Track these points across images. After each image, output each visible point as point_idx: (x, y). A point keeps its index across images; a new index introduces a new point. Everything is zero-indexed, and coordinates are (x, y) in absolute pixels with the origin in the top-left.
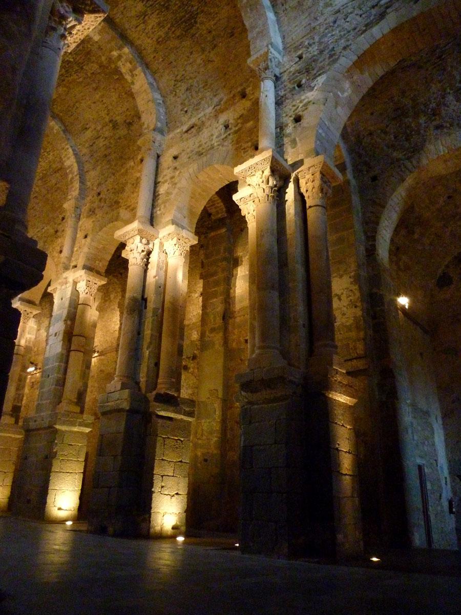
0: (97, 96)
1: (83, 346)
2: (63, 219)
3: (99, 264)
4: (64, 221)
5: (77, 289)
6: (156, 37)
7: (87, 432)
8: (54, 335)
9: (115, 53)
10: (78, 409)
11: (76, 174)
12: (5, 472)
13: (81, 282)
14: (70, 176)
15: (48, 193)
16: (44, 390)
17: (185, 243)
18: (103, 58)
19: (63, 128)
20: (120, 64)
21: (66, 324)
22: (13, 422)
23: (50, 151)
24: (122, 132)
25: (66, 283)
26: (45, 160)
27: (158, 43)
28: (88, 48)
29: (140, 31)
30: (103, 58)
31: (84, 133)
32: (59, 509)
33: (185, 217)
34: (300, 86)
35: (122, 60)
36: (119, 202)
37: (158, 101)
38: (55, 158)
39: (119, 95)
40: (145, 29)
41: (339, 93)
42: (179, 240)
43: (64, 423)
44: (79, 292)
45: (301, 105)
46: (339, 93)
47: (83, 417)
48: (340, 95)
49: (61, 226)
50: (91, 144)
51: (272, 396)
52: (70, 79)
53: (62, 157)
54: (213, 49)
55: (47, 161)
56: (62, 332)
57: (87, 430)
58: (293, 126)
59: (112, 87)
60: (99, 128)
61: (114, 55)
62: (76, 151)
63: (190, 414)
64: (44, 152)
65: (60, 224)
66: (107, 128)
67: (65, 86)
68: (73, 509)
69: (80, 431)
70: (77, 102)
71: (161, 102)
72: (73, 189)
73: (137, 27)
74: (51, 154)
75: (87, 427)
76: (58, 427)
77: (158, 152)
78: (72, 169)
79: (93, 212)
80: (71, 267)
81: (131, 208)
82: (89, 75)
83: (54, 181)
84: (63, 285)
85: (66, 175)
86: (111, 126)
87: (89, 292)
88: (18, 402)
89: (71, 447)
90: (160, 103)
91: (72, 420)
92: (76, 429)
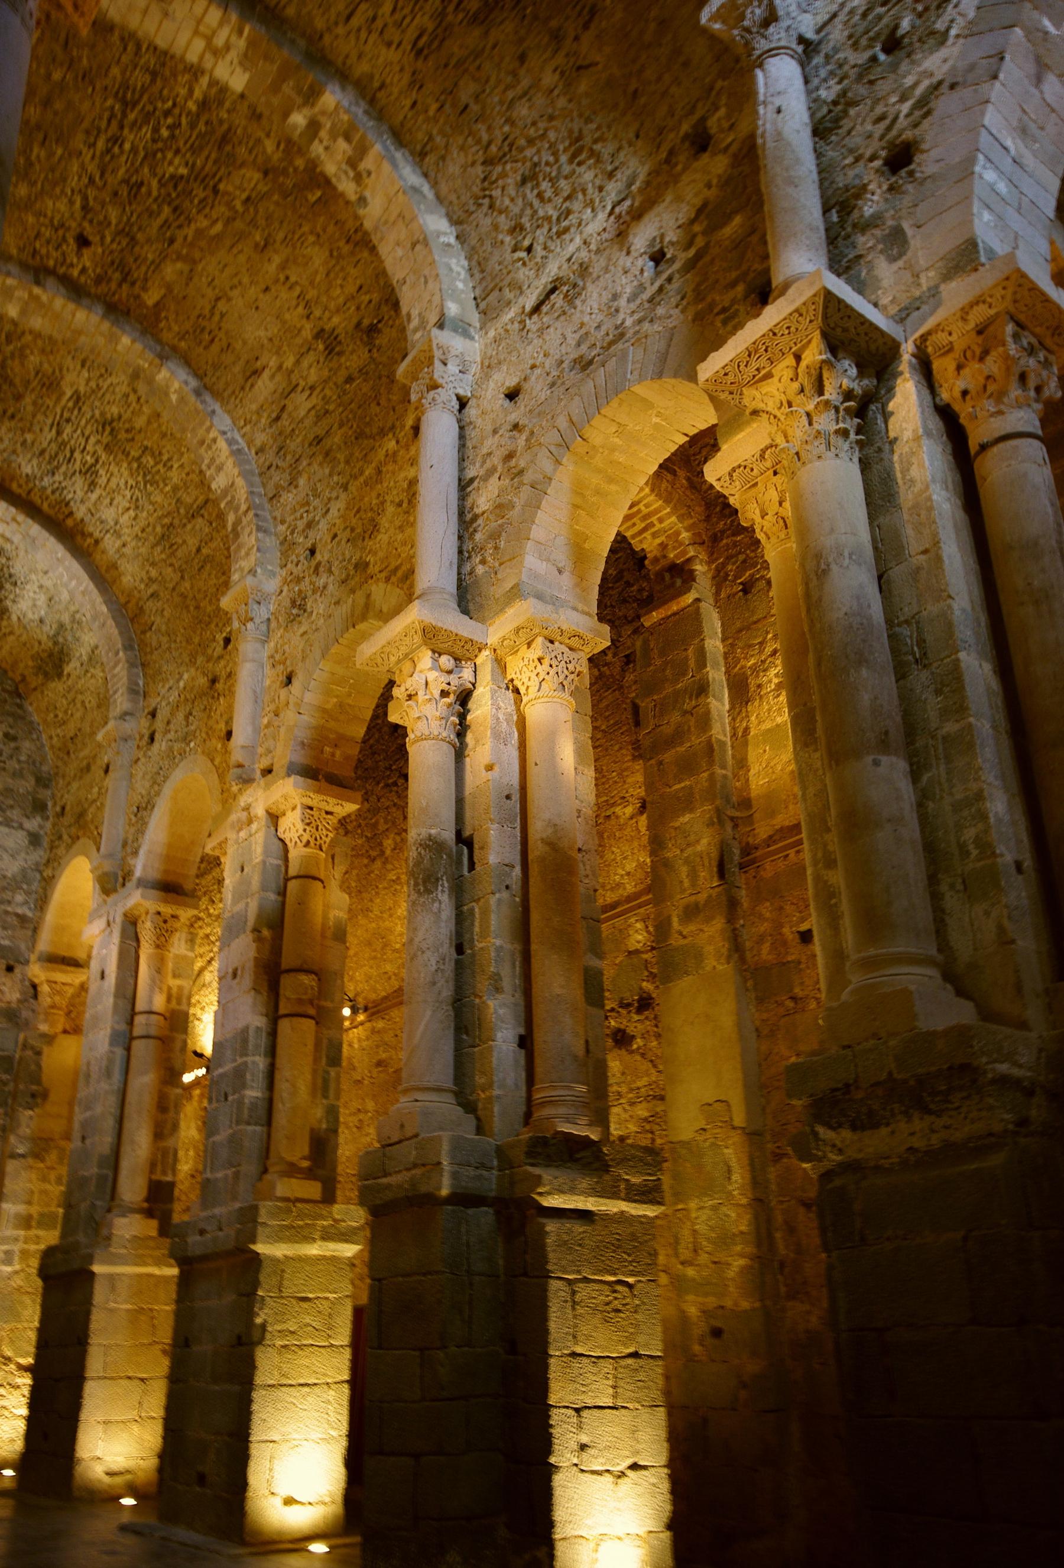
0: (272, 268)
1: (311, 1002)
2: (227, 641)
3: (333, 755)
4: (230, 647)
5: (282, 836)
6: (411, 34)
7: (349, 1254)
8: (230, 976)
9: (298, 119)
10: (313, 1189)
11: (244, 507)
12: (142, 1380)
13: (289, 814)
14: (231, 518)
15: (182, 577)
16: (217, 1138)
17: (571, 649)
18: (269, 146)
19: (193, 383)
20: (317, 149)
21: (259, 940)
22: (154, 1233)
23: (169, 459)
24: (355, 358)
25: (250, 822)
26: (161, 485)
27: (419, 52)
28: (221, 122)
29: (359, 30)
30: (269, 146)
31: (252, 386)
32: (289, 1501)
33: (560, 572)
34: (893, 44)
35: (323, 134)
36: (367, 564)
37: (443, 239)
38: (188, 474)
39: (331, 251)
40: (374, 19)
41: (1047, 23)
42: (552, 642)
43: (282, 1235)
44: (287, 842)
45: (905, 108)
46: (1047, 23)
47: (330, 1213)
48: (1051, 29)
49: (222, 663)
50: (274, 415)
51: (935, 1140)
52: (190, 231)
53: (204, 467)
54: (586, 26)
55: (168, 489)
56: (250, 965)
57: (349, 1250)
58: (885, 187)
59: (306, 228)
60: (289, 363)
61: (295, 126)
62: (237, 443)
63: (648, 1194)
64: (157, 463)
65: (220, 657)
66: (311, 357)
67: (179, 257)
68: (327, 1499)
69: (328, 1254)
70: (218, 299)
71: (452, 240)
72: (243, 552)
73: (349, 18)
74: (176, 466)
75: (347, 1241)
76: (260, 1248)
77: (461, 392)
78: (233, 497)
79: (302, 608)
80: (258, 773)
81: (400, 573)
82: (239, 207)
83: (192, 542)
84: (241, 829)
85: (221, 516)
86: (321, 347)
87: (312, 842)
88: (164, 1173)
89: (305, 1305)
90: (449, 245)
91: (301, 1223)
92: (314, 1250)
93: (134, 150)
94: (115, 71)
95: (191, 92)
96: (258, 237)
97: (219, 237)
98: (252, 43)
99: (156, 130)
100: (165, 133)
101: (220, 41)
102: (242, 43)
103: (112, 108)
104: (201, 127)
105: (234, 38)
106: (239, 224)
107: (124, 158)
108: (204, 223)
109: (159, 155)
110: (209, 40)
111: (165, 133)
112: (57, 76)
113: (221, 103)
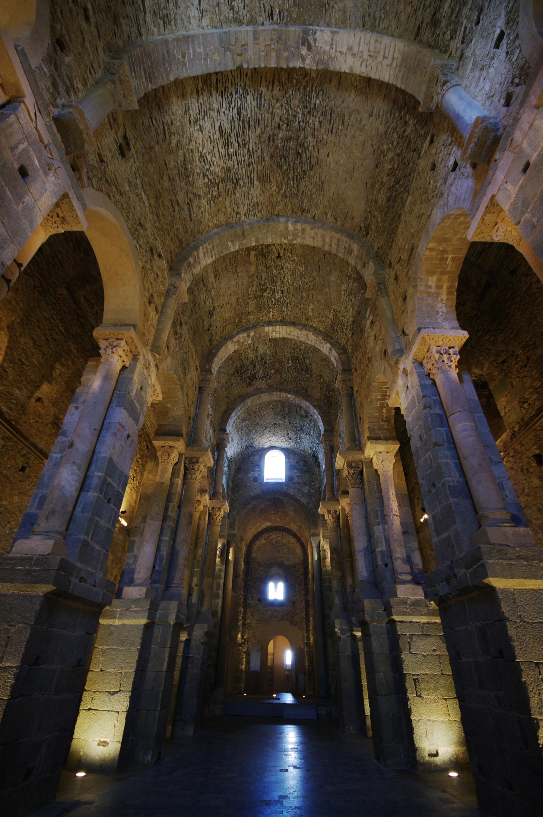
6: (243, 354)
31: (214, 273)
52: (255, 284)
67: (253, 275)
93: (278, 292)
94: (290, 309)
97: (248, 290)
98: (268, 336)
99: (275, 299)
100: (273, 299)
101: (274, 333)
103: (287, 299)
104: (266, 307)
106: (246, 297)
108: (254, 289)
110: (276, 332)
111: (273, 299)
112: (302, 305)
113: (266, 315)
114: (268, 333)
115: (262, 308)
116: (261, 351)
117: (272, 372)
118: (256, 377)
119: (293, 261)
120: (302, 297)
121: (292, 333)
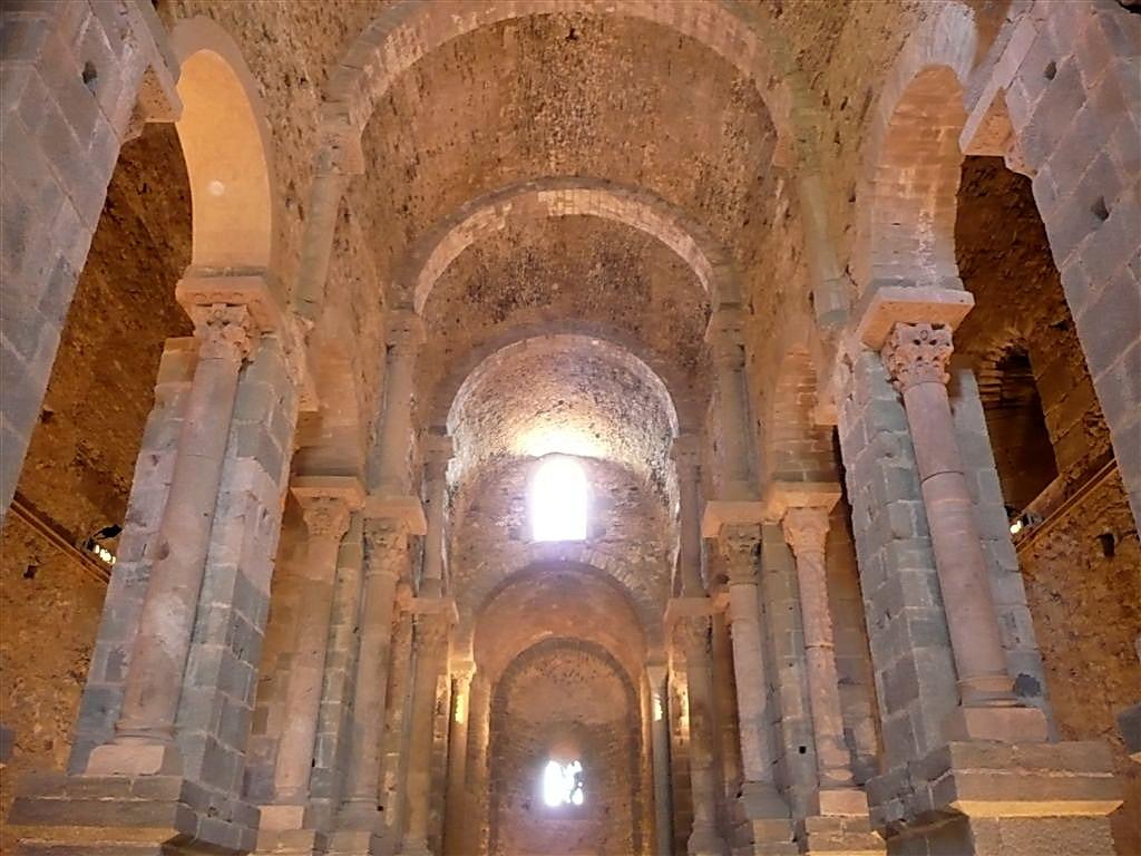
6: (485, 251)
52: (514, 96)
67: (510, 78)
93: (569, 113)
95: (556, 157)
96: (480, 134)
97: (498, 111)
99: (563, 128)
100: (557, 129)
102: (550, 209)
104: (542, 145)
105: (555, 208)
107: (573, 106)
108: (511, 107)
109: (554, 116)
112: (627, 144)
114: (545, 204)
115: (532, 149)
116: (528, 242)
117: (555, 286)
118: (514, 300)
119: (606, 47)
120: (628, 127)
121: (602, 205)
